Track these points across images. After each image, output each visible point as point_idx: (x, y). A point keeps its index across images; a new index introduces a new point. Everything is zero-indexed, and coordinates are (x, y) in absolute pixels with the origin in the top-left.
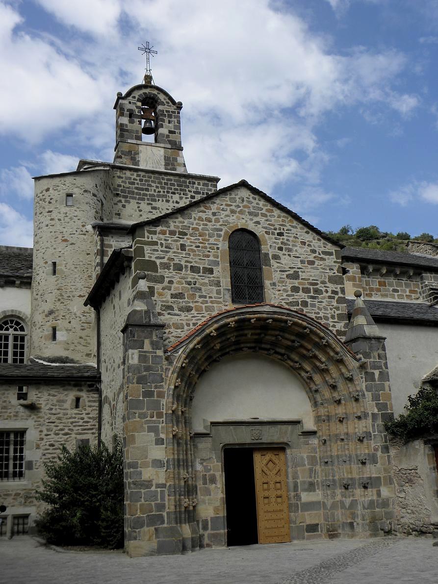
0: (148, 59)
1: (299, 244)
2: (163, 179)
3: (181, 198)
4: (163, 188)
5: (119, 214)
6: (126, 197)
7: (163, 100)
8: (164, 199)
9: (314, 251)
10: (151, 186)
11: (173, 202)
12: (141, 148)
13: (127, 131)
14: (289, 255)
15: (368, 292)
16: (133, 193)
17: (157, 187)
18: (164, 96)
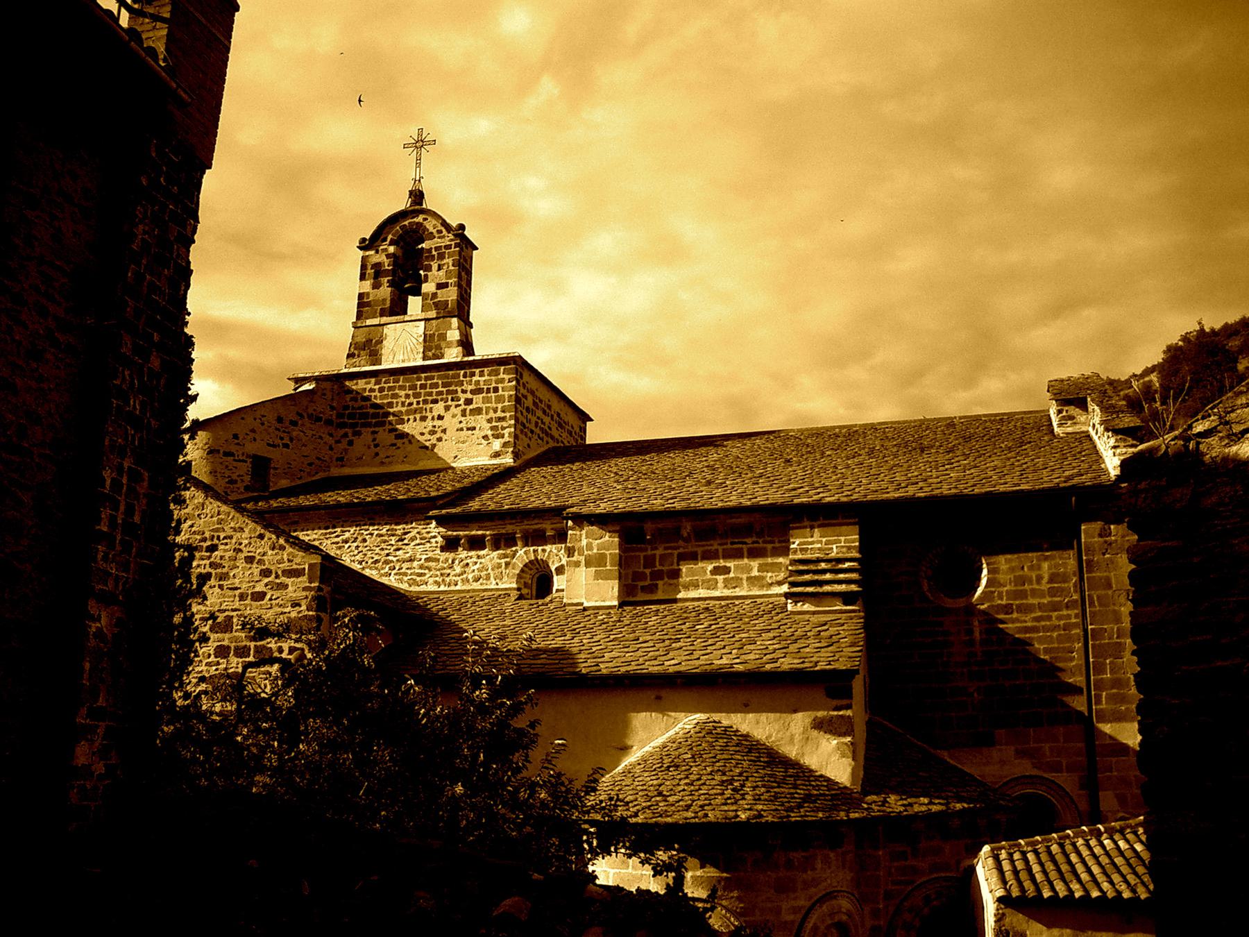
0: (419, 159)
1: (241, 563)
2: (419, 379)
3: (447, 408)
4: (416, 395)
5: (341, 459)
6: (353, 426)
7: (431, 229)
8: (418, 416)
9: (266, 573)
10: (395, 396)
11: (433, 419)
12: (386, 330)
13: (368, 304)
14: (221, 587)
15: (648, 582)
16: (366, 415)
17: (407, 396)
18: (434, 222)
